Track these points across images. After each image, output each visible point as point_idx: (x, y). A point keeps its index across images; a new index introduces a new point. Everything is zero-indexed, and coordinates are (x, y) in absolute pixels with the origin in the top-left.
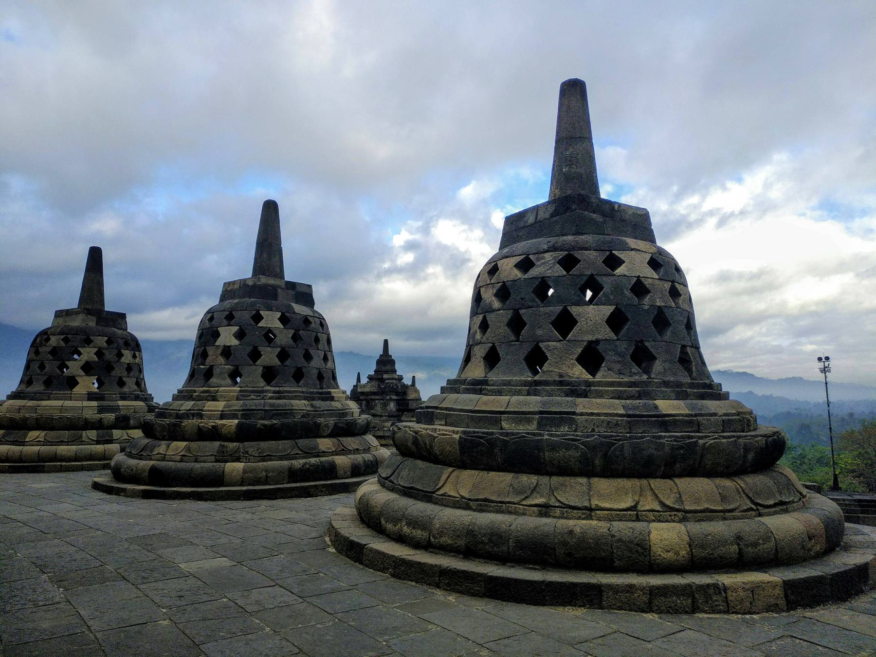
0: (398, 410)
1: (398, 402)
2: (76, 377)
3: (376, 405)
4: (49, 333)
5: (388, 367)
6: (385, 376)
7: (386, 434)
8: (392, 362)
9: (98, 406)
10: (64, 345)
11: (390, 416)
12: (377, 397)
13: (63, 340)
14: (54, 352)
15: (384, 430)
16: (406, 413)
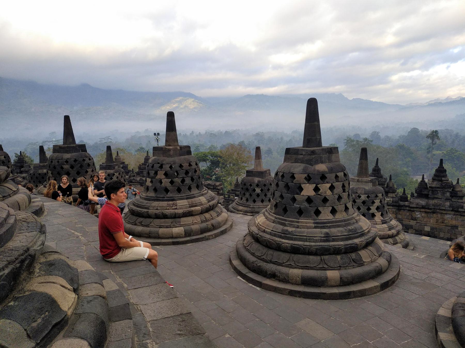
0: (450, 196)
1: (451, 193)
2: (375, 214)
3: (438, 193)
4: (359, 192)
5: (444, 174)
6: (443, 179)
7: (447, 209)
8: (445, 171)
9: (388, 227)
10: (368, 200)
11: (447, 199)
12: (440, 190)
13: (367, 197)
14: (364, 202)
15: (445, 207)
16: (454, 197)
